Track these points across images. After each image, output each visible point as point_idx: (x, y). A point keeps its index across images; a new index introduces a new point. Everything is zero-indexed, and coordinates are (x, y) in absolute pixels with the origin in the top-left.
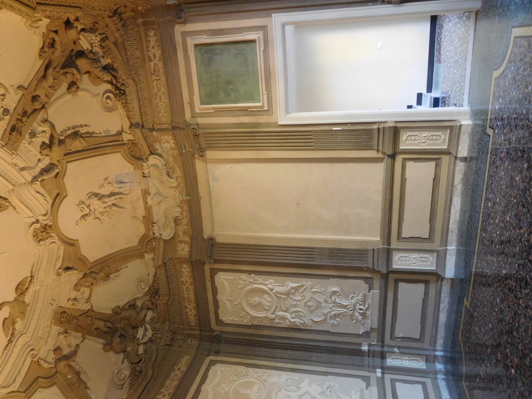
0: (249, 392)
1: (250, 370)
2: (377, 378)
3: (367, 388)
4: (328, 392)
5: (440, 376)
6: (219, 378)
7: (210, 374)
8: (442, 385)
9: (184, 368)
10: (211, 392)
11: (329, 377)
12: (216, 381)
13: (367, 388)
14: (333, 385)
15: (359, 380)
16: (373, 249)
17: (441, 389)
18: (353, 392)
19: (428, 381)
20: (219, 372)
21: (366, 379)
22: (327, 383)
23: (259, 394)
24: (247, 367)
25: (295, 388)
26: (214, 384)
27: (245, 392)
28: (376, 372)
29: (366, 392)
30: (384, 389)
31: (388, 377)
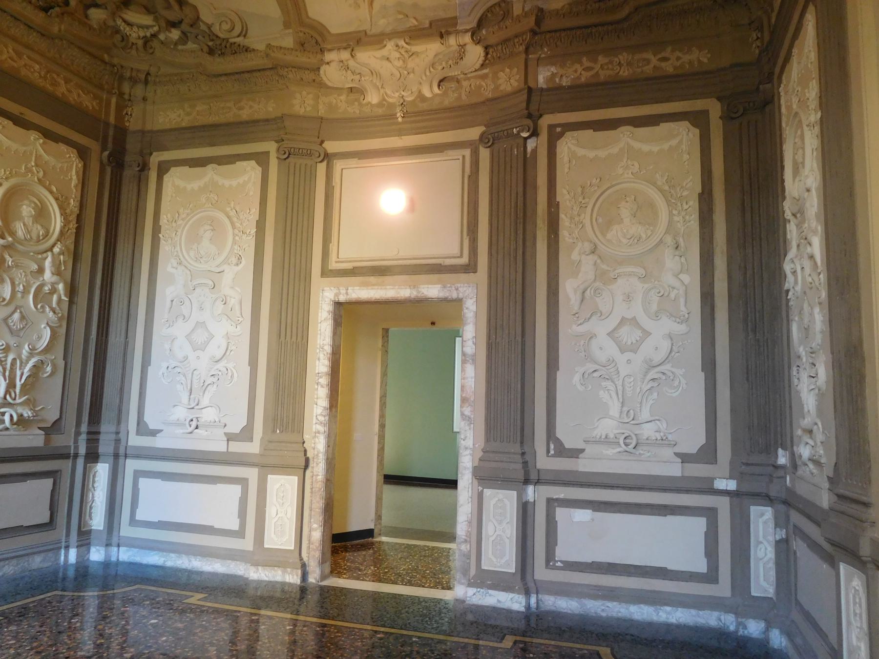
0: (627, 221)
1: (693, 204)
2: (712, 480)
3: (676, 454)
4: (652, 374)
5: (729, 621)
6: (655, 149)
7: (665, 127)
8: (710, 619)
9: (668, 68)
10: (615, 150)
11: (700, 377)
12: (646, 148)
13: (676, 454)
14: (676, 383)
15: (702, 440)
16: (866, 505)
17: (693, 612)
18: (663, 426)
19: (723, 589)
20: (674, 142)
21: (708, 453)
22: (679, 372)
23: (625, 241)
24: (701, 195)
25: (654, 307)
26: (636, 145)
27: (625, 212)
28: (731, 477)
29: (668, 453)
30: (665, 490)
31: (723, 505)
